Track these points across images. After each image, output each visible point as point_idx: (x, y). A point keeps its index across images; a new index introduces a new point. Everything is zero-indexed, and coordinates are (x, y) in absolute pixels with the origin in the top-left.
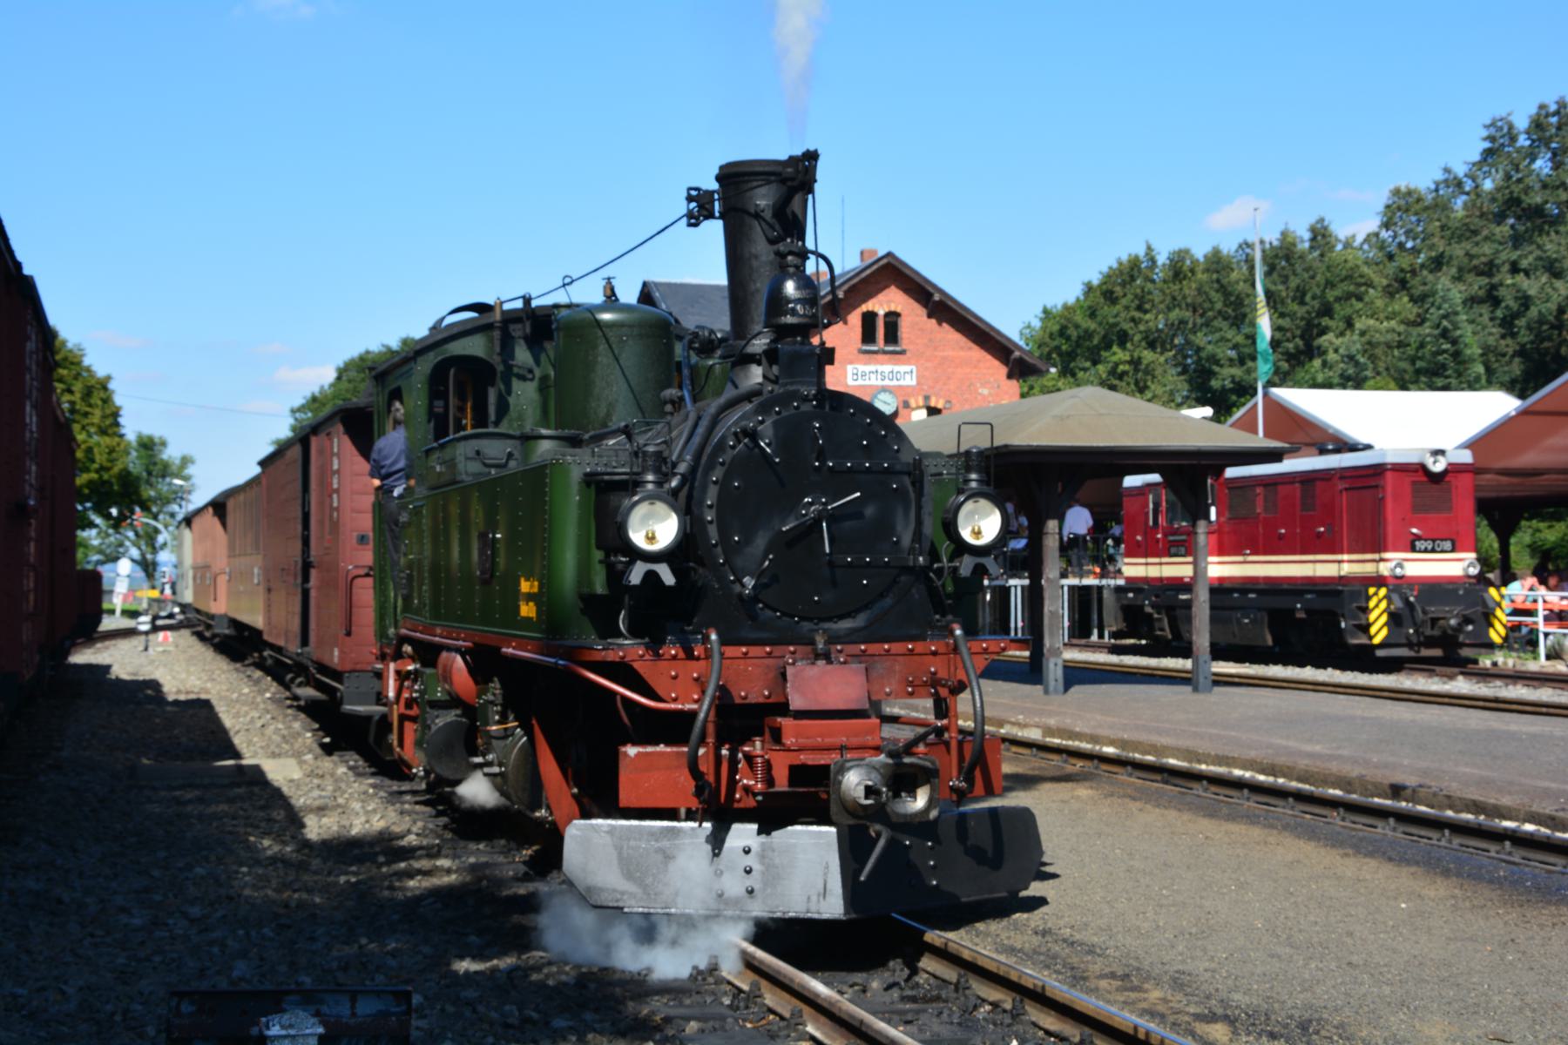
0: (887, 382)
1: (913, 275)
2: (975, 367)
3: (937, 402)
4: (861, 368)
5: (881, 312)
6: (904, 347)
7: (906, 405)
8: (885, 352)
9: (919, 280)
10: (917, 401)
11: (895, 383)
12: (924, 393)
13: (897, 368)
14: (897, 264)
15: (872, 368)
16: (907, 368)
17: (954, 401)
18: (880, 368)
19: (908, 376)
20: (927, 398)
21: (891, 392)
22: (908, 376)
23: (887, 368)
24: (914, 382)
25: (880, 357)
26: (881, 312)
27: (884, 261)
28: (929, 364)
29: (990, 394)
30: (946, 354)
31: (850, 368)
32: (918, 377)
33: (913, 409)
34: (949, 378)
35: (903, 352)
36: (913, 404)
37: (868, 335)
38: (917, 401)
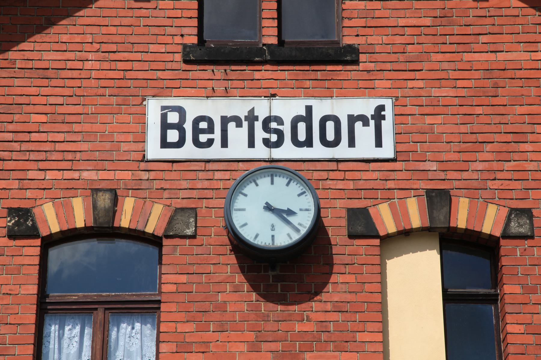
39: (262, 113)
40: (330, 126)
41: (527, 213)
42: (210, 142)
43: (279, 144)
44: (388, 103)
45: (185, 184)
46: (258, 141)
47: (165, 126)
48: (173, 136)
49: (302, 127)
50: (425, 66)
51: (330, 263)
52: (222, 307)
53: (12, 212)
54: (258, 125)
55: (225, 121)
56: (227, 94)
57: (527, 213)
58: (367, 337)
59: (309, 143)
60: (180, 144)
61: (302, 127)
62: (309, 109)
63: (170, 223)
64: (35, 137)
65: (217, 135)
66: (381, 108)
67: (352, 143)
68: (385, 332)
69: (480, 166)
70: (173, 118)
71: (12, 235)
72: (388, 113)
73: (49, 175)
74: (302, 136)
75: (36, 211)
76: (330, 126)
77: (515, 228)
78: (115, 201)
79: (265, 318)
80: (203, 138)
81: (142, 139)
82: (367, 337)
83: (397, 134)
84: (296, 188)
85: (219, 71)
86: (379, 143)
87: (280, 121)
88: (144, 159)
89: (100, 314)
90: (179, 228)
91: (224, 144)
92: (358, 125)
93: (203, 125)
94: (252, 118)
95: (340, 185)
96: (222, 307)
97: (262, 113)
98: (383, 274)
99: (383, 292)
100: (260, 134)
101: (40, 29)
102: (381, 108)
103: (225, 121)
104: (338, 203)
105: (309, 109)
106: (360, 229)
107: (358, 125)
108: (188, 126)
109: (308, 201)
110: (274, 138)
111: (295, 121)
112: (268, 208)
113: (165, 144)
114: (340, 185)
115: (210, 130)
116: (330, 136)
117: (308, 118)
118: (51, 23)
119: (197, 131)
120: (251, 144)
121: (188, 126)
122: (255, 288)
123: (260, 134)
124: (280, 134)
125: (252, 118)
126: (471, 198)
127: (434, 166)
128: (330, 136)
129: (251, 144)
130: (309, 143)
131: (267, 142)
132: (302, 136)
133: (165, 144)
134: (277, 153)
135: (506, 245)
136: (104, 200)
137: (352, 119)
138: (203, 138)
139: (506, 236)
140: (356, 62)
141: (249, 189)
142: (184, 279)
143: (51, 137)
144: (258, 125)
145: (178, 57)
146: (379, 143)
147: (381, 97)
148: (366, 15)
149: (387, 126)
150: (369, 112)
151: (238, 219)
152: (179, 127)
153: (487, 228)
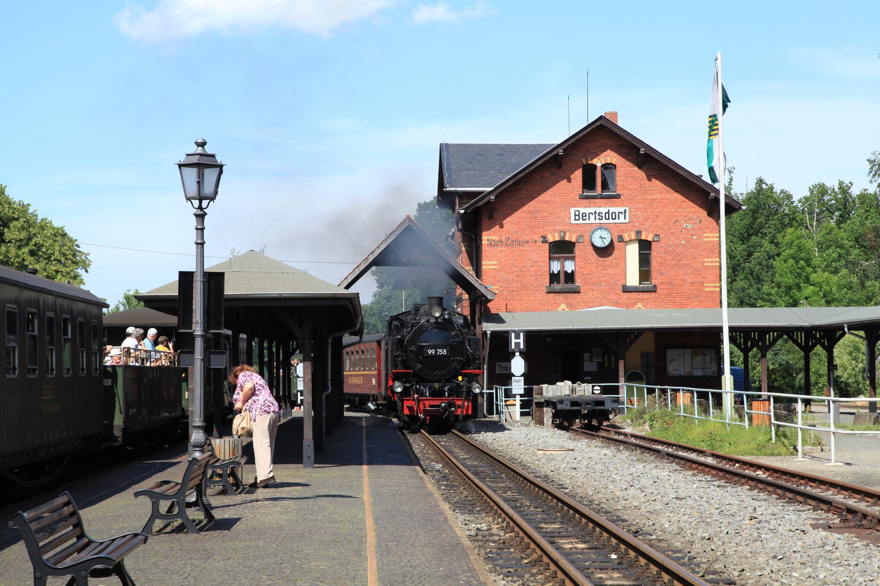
0: (604, 221)
1: (623, 134)
2: (680, 207)
3: (647, 236)
4: (582, 210)
5: (599, 165)
6: (618, 192)
7: (621, 239)
8: (602, 197)
9: (628, 138)
10: (629, 236)
11: (611, 221)
12: (636, 229)
13: (612, 210)
14: (609, 126)
15: (592, 210)
16: (622, 209)
17: (661, 235)
18: (598, 210)
19: (622, 216)
20: (639, 233)
21: (605, 229)
22: (622, 216)
23: (604, 210)
24: (627, 221)
25: (598, 201)
26: (599, 165)
27: (599, 123)
28: (639, 206)
29: (693, 228)
30: (654, 196)
31: (572, 210)
32: (630, 218)
33: (627, 243)
34: (657, 217)
35: (618, 197)
36: (627, 239)
37: (588, 183)
38: (629, 236)
39: (598, 212)
40: (614, 214)
41: (658, 235)
42: (586, 219)
43: (602, 219)
44: (627, 208)
45: (580, 229)
46: (597, 219)
47: (575, 215)
48: (577, 218)
49: (607, 215)
50: (636, 198)
51: (614, 248)
52: (589, 259)
53: (542, 237)
54: (597, 215)
55: (589, 214)
56: (589, 207)
57: (658, 235)
58: (622, 265)
59: (609, 219)
60: (579, 220)
61: (607, 215)
62: (609, 210)
63: (577, 239)
64: (546, 218)
65: (587, 217)
66: (626, 210)
67: (619, 219)
68: (625, 264)
69: (648, 224)
70: (577, 213)
71: (543, 242)
72: (627, 211)
73: (549, 228)
74: (607, 217)
75: (547, 237)
76: (614, 214)
77: (655, 239)
78: (565, 234)
79: (599, 261)
80: (584, 218)
81: (570, 218)
82: (622, 265)
83: (629, 216)
84: (606, 232)
85: (587, 200)
86: (625, 219)
87: (602, 214)
88: (570, 223)
89: (562, 260)
90: (579, 240)
91: (589, 219)
92: (620, 214)
93: (584, 215)
94: (595, 213)
95: (616, 229)
96: (589, 259)
97: (598, 212)
98: (625, 248)
99: (625, 255)
100: (597, 217)
101: (546, 191)
102: (626, 210)
103: (589, 214)
104: (616, 234)
105: (609, 210)
106: (620, 240)
107: (620, 214)
108: (581, 215)
109: (609, 235)
110: (601, 218)
111: (606, 213)
112: (601, 237)
113: (575, 220)
114: (616, 229)
115: (586, 216)
116: (614, 217)
117: (608, 213)
118: (548, 189)
119: (583, 216)
120: (595, 219)
121: (581, 215)
122: (597, 254)
123: (597, 217)
124: (602, 217)
125: (595, 213)
126: (646, 231)
127: (638, 224)
128: (614, 217)
129: (595, 219)
130: (609, 219)
131: (599, 219)
132: (607, 217)
133: (575, 220)
134: (601, 222)
135: (653, 243)
136: (562, 234)
137: (619, 213)
138: (584, 218)
139: (653, 241)
140: (620, 198)
141: (596, 232)
142: (581, 252)
143: (549, 218)
144: (597, 215)
145: (578, 197)
146: (625, 219)
147: (626, 206)
148: (622, 185)
149: (627, 214)
150: (623, 211)
151: (593, 240)
152: (578, 215)
153: (649, 239)
